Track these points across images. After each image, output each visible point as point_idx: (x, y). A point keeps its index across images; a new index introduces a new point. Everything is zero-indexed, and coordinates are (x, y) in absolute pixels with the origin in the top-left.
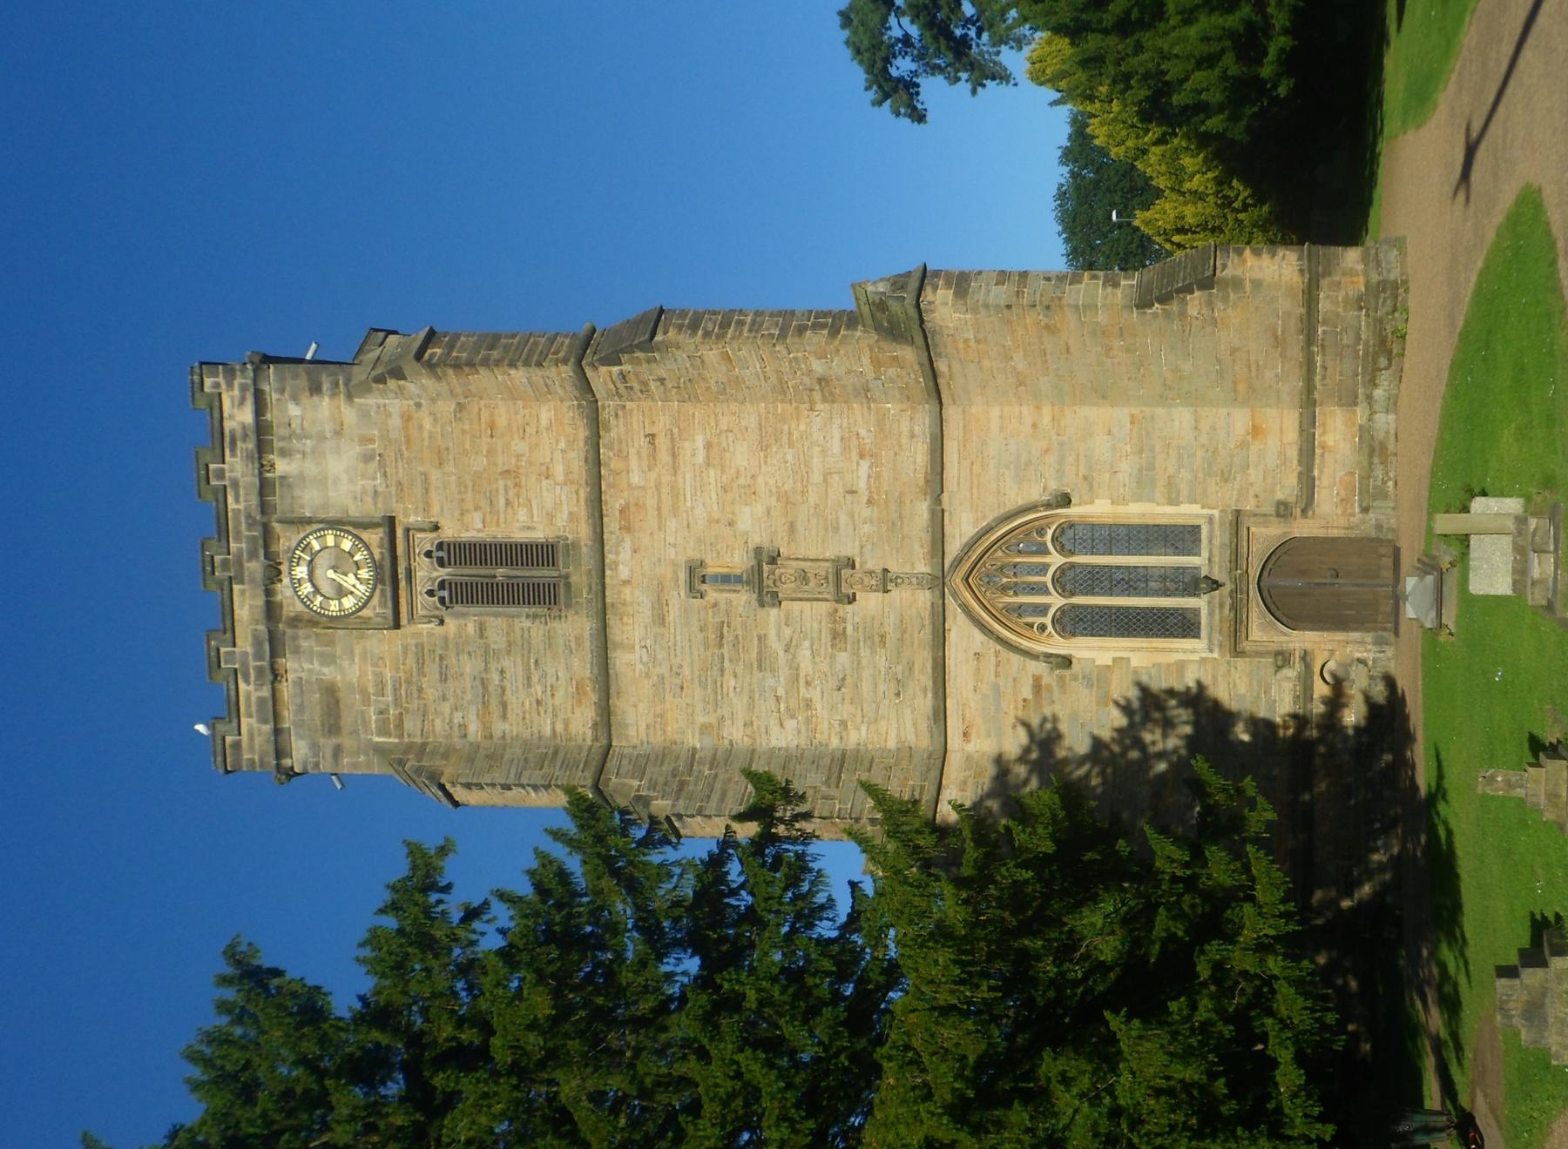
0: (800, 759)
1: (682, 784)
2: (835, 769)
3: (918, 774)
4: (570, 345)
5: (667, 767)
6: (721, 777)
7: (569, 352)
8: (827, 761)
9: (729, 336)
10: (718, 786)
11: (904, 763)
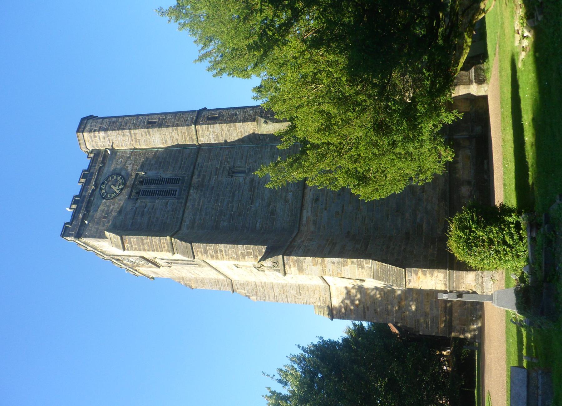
0: (286, 286)
1: (256, 293)
2: (298, 290)
3: (323, 293)
4: (167, 244)
5: (250, 287)
6: (266, 291)
7: (168, 246)
8: (295, 287)
9: (219, 257)
10: (266, 294)
11: (318, 289)
